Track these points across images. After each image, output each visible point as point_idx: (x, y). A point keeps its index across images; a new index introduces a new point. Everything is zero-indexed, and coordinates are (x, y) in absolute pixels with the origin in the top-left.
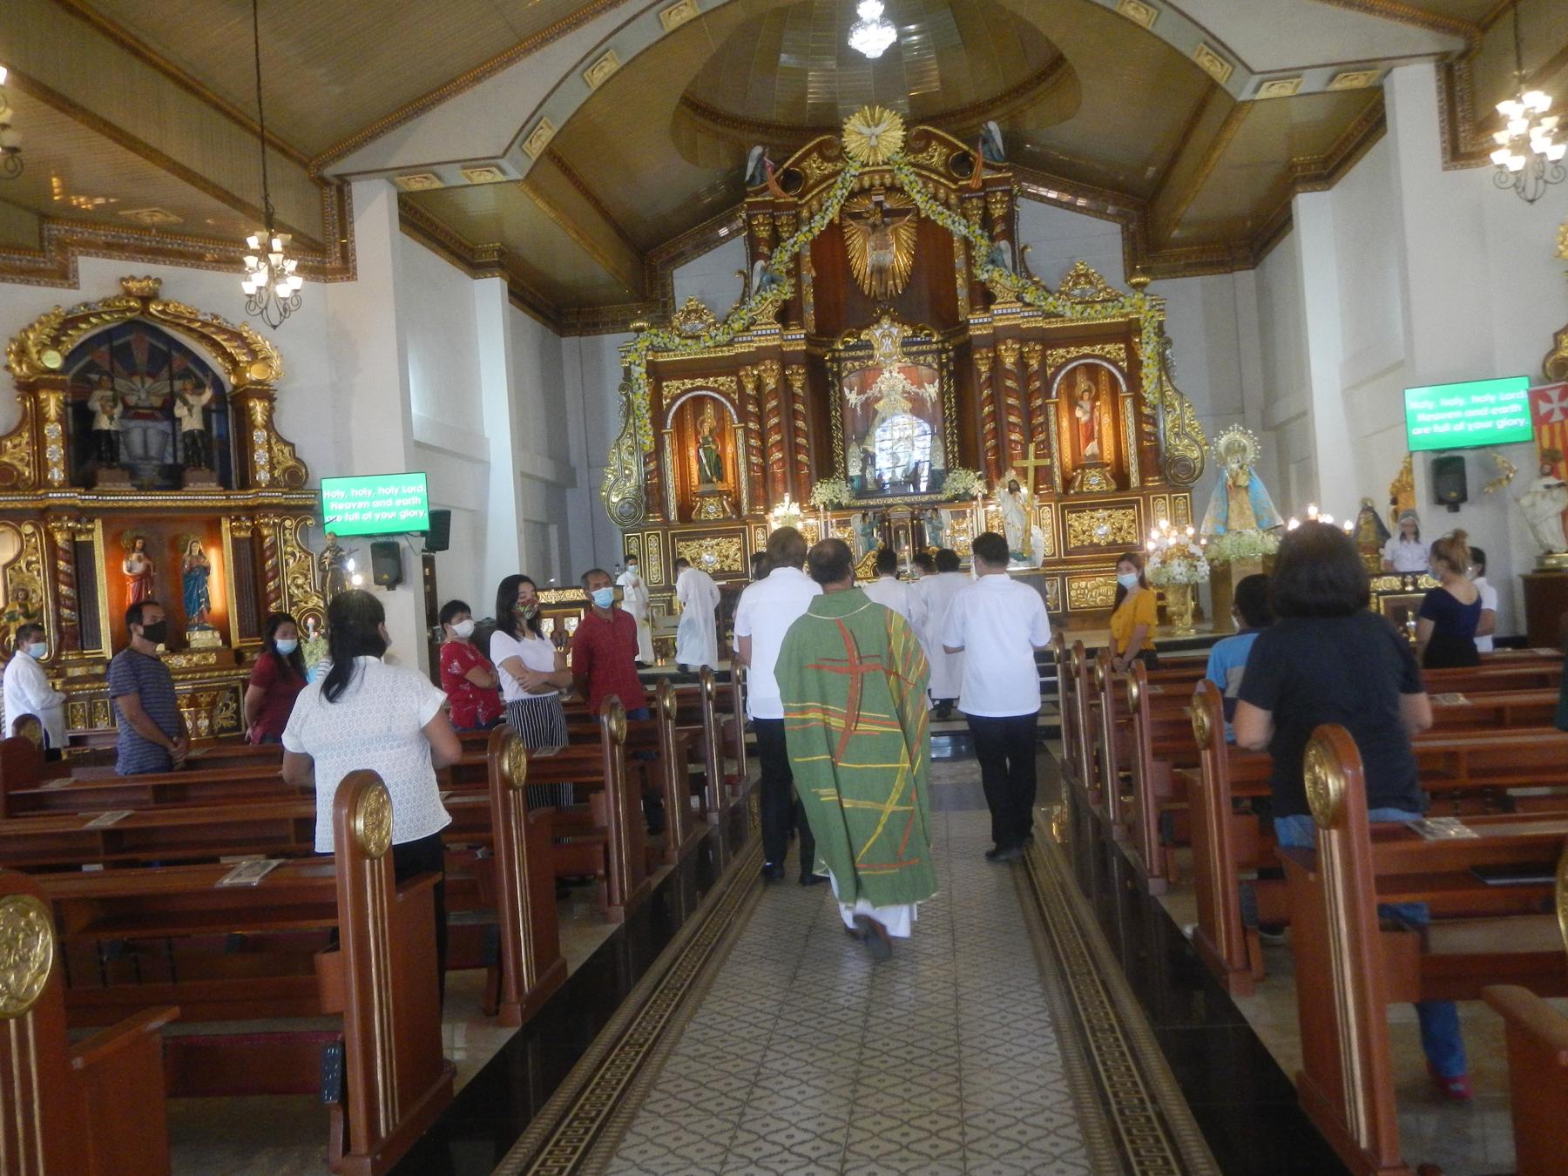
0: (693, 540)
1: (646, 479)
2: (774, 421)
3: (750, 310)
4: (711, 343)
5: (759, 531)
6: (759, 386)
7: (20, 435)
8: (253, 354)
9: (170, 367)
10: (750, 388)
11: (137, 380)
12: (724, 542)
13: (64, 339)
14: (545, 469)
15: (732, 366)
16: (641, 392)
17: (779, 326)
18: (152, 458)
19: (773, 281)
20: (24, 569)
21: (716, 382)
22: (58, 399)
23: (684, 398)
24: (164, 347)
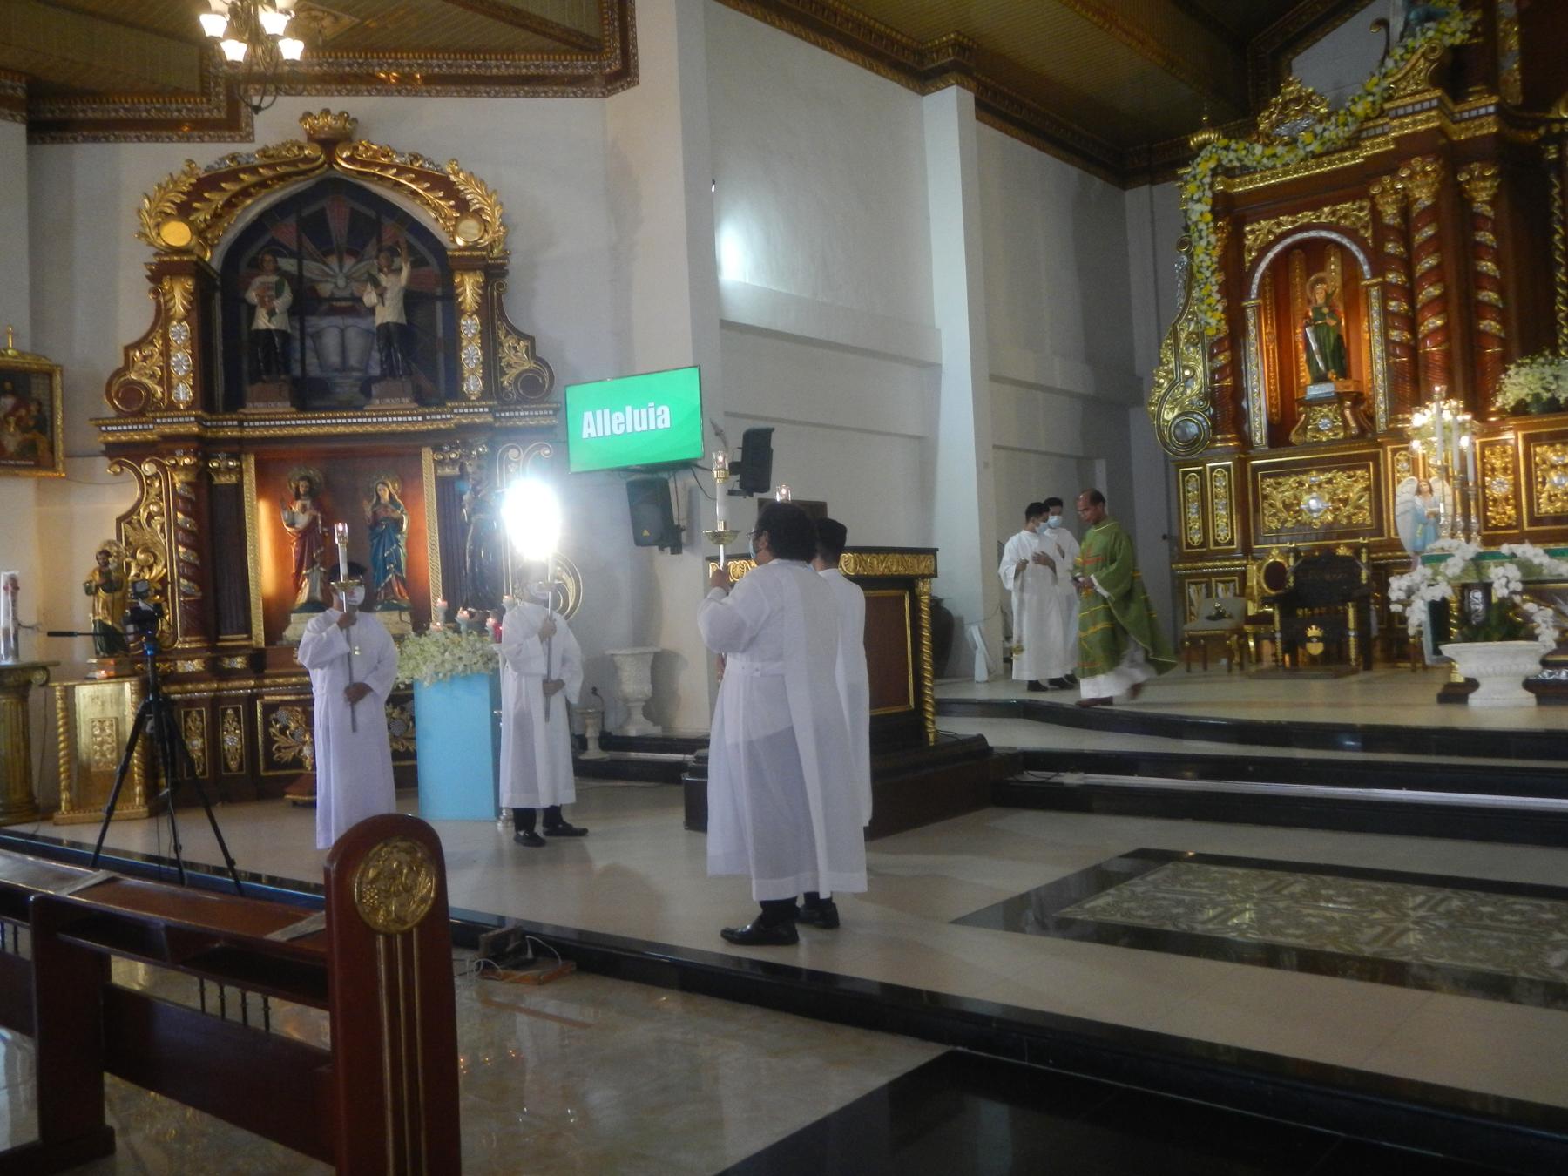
0: (1289, 475)
1: (1213, 381)
2: (1429, 262)
3: (1385, 76)
4: (1315, 147)
5: (1400, 456)
6: (1405, 212)
7: (152, 343)
8: (463, 206)
9: (379, 240)
10: (1390, 213)
11: (333, 261)
12: (1341, 479)
13: (196, 205)
14: (1066, 373)
15: (1352, 184)
16: (1204, 243)
17: (1438, 92)
18: (353, 369)
19: (1430, 17)
20: (144, 522)
21: (1333, 213)
22: (185, 289)
23: (1278, 248)
24: (372, 213)
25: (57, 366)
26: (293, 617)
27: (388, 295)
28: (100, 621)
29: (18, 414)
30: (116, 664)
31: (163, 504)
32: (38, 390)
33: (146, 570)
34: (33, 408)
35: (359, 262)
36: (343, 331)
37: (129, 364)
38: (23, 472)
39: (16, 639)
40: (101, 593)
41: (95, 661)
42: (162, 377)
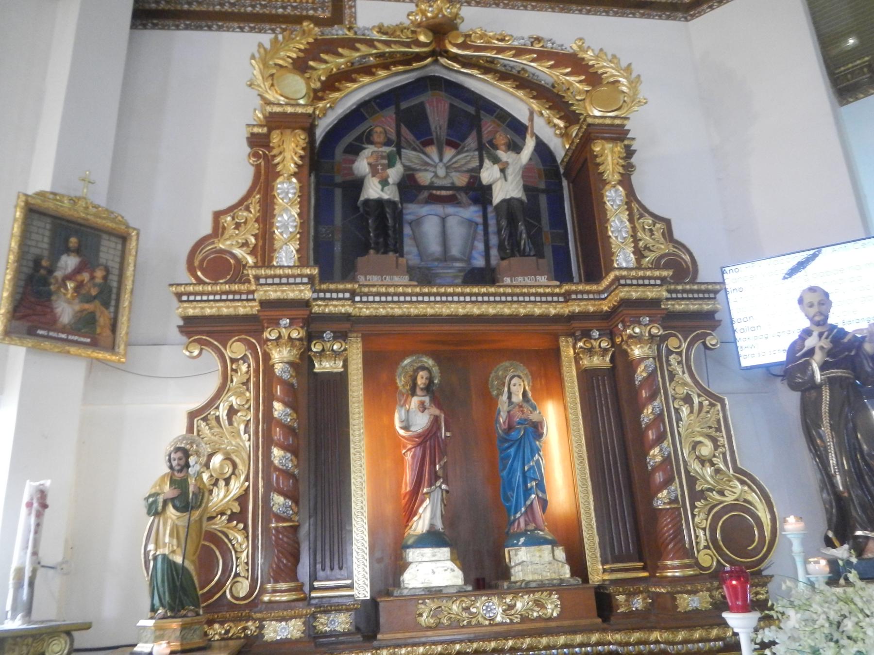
7: (247, 209)
11: (432, 151)
13: (311, 63)
18: (456, 259)
24: (471, 110)
25: (134, 229)
26: (413, 555)
27: (509, 171)
28: (164, 556)
29: (79, 278)
30: (184, 627)
31: (251, 395)
32: (108, 252)
33: (222, 483)
34: (99, 274)
35: (458, 153)
36: (443, 220)
37: (218, 230)
38: (73, 350)
39: (31, 584)
40: (171, 511)
41: (151, 623)
42: (256, 246)
